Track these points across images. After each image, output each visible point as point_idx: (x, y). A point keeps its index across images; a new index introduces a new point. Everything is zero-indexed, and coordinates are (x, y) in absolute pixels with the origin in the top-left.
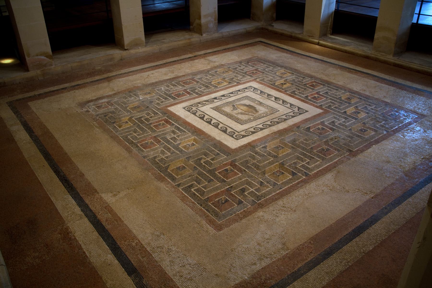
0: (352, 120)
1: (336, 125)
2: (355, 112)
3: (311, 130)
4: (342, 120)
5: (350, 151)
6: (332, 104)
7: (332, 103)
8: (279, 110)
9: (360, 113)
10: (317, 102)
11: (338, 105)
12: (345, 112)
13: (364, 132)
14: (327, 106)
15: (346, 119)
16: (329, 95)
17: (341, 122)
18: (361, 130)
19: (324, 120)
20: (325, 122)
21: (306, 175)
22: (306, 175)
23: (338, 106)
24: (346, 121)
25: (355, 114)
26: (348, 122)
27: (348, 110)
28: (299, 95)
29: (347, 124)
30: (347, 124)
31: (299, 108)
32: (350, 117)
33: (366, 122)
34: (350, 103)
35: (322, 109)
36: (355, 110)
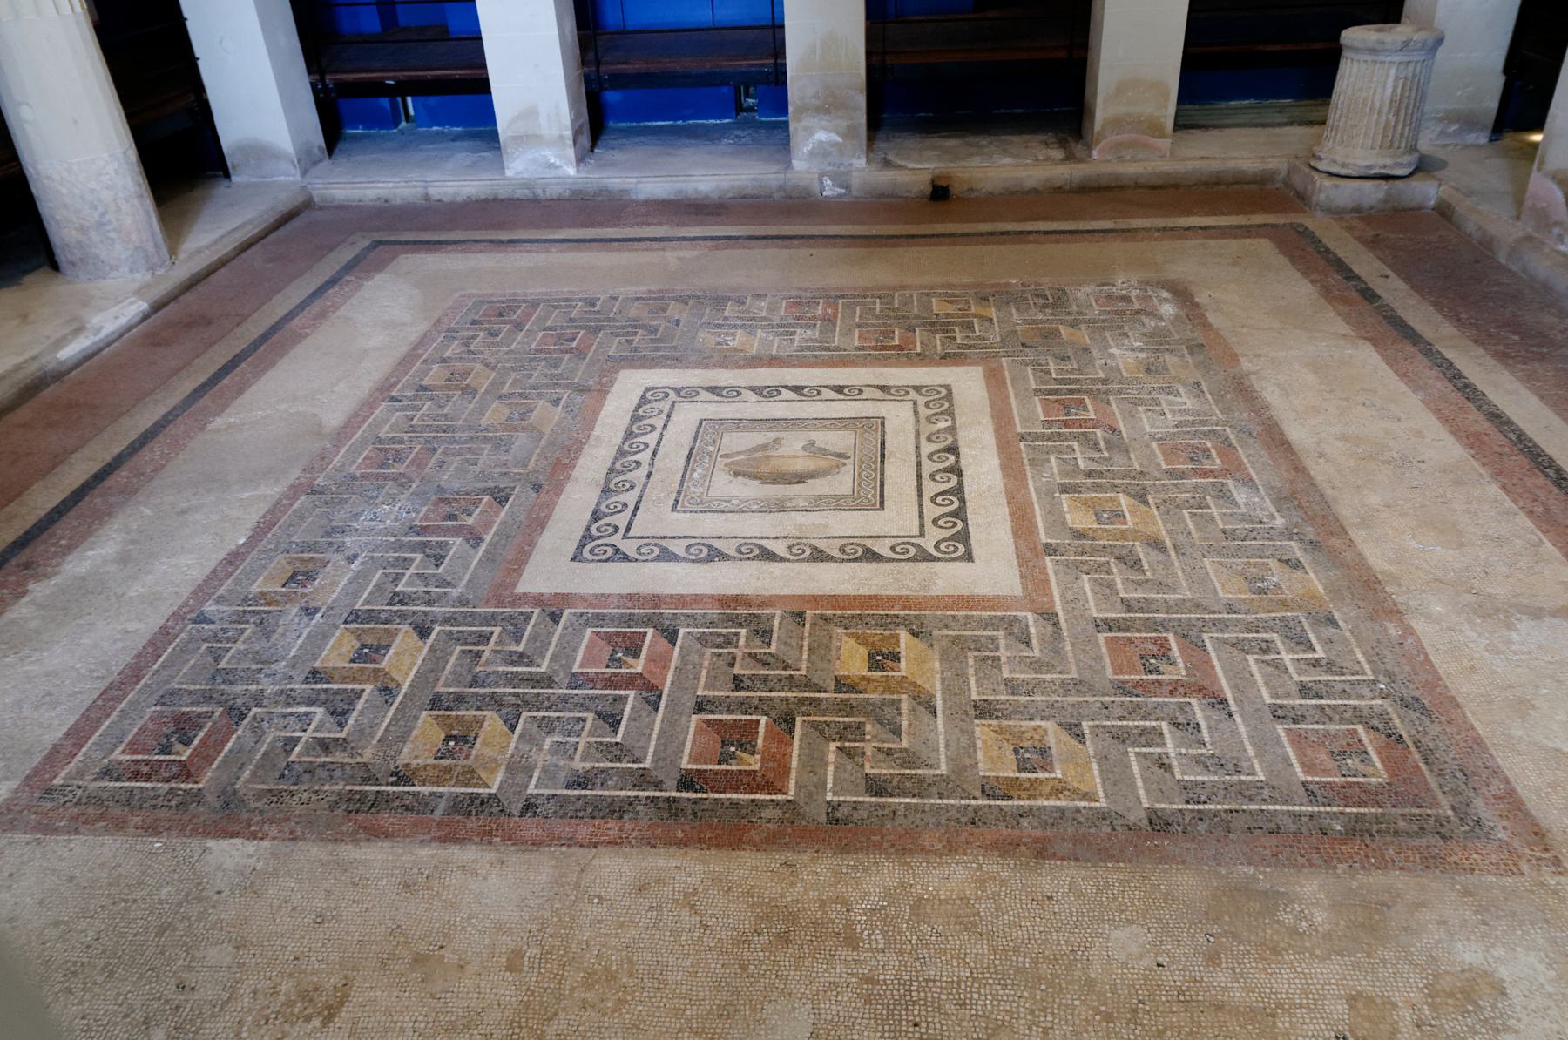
0: (367, 602)
1: (414, 551)
2: (380, 649)
3: (487, 498)
4: (407, 584)
5: (314, 492)
6: (514, 648)
7: (521, 655)
8: (675, 514)
9: (353, 661)
10: (587, 624)
11: (484, 659)
12: (423, 632)
13: (295, 574)
14: (529, 628)
15: (395, 594)
16: (582, 707)
17: (408, 573)
18: (310, 576)
19: (480, 553)
20: (467, 546)
21: (393, 399)
22: (393, 399)
23: (478, 655)
24: (390, 588)
25: (369, 640)
26: (378, 587)
27: (419, 650)
28: (712, 624)
29: (377, 576)
30: (377, 576)
31: (620, 556)
32: (383, 616)
33: (306, 619)
34: (436, 703)
35: (538, 600)
36: (384, 665)
